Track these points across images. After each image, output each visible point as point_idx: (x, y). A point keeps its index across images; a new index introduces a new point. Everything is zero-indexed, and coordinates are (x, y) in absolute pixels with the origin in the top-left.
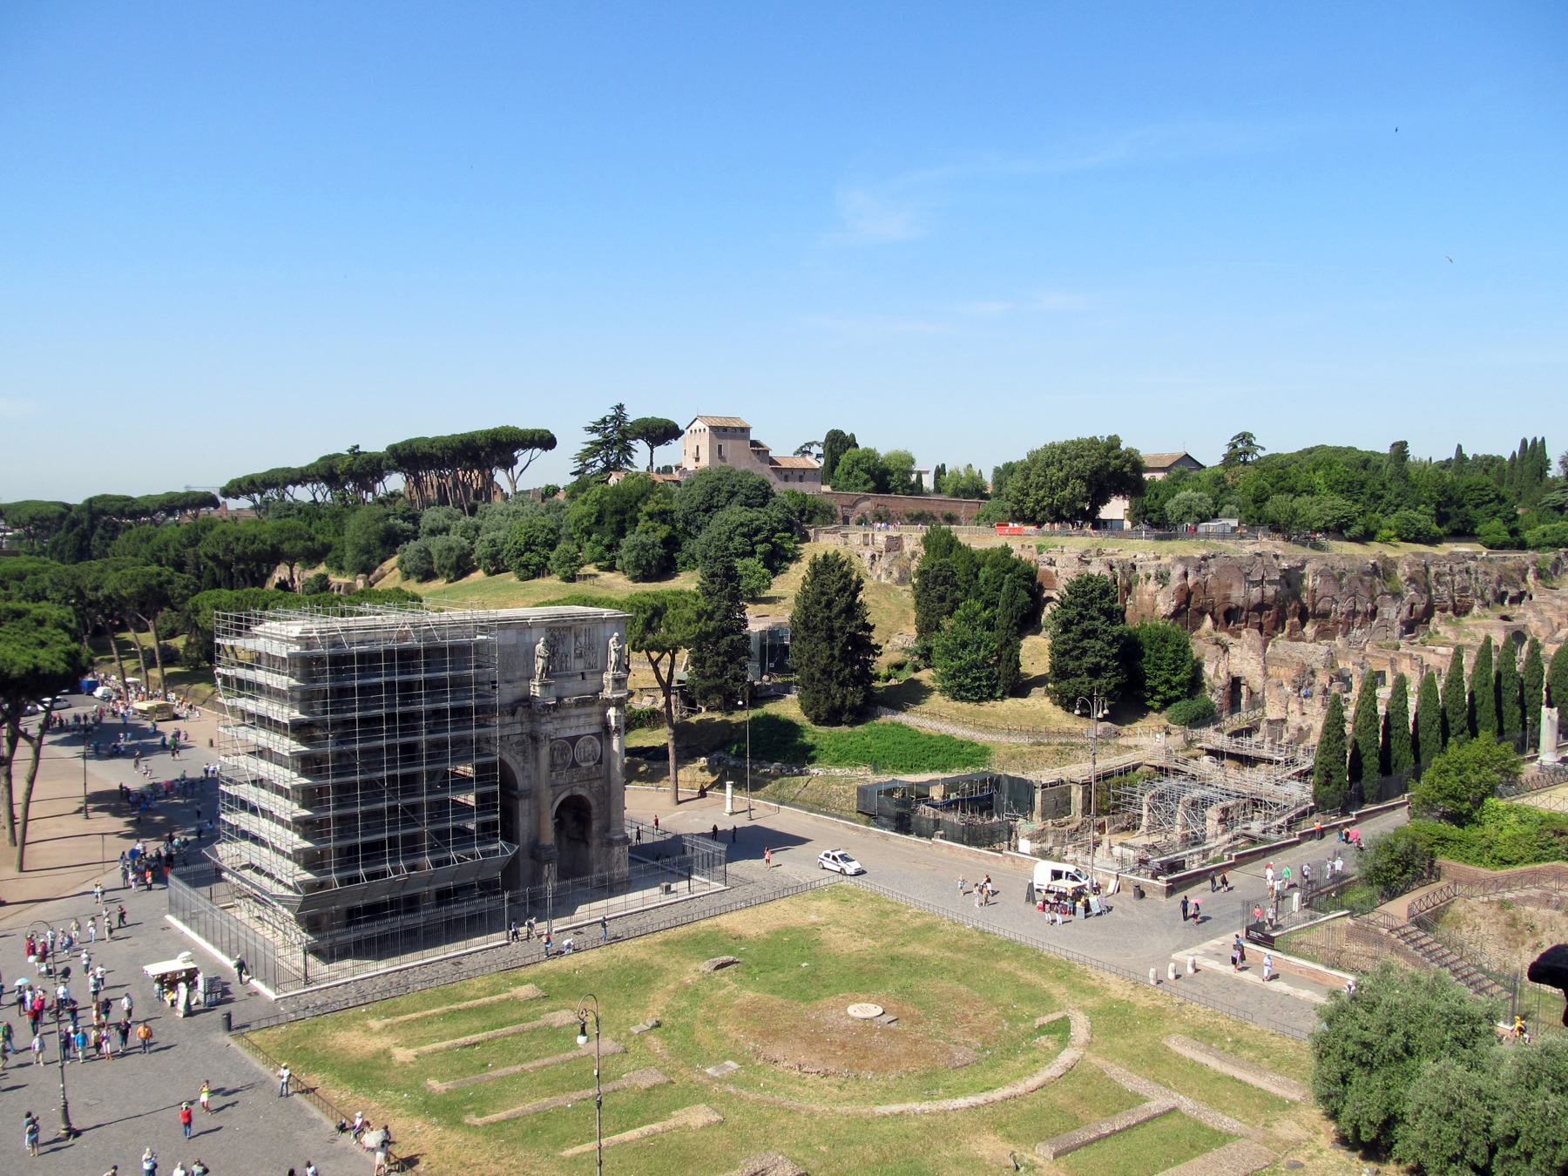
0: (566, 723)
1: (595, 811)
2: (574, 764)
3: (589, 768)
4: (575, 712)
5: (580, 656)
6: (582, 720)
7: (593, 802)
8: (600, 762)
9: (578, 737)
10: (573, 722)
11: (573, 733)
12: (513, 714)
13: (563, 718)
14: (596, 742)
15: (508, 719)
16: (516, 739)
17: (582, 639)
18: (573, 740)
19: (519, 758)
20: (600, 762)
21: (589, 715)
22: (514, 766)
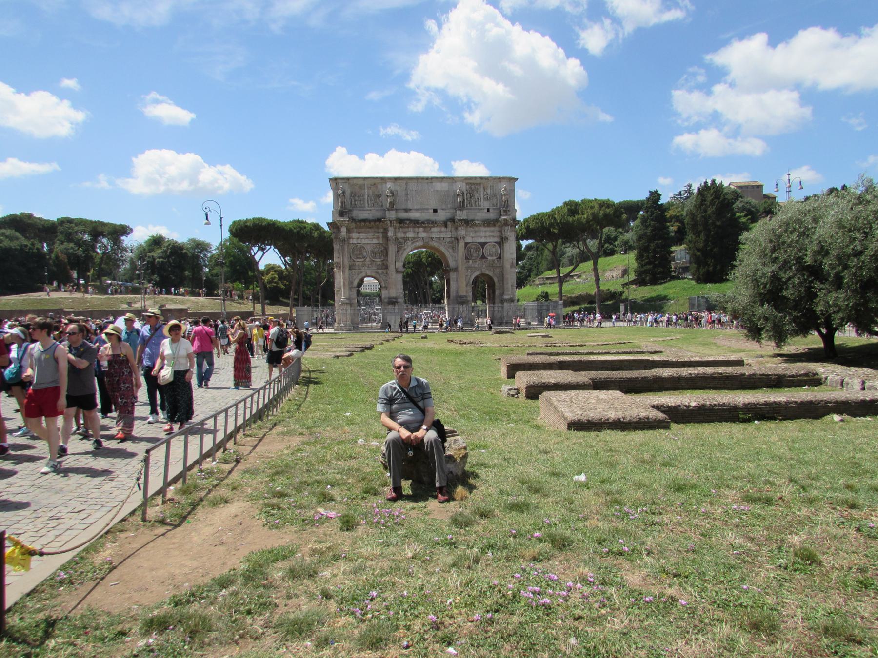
0: (478, 234)
1: (496, 284)
2: (483, 257)
3: (493, 261)
4: (483, 229)
5: (488, 199)
6: (488, 234)
7: (495, 280)
8: (500, 257)
9: (485, 243)
10: (482, 234)
11: (483, 240)
12: (446, 226)
13: (476, 232)
14: (497, 246)
15: (443, 229)
16: (448, 240)
17: (489, 191)
18: (483, 244)
19: (450, 250)
20: (500, 257)
21: (493, 232)
22: (447, 254)
